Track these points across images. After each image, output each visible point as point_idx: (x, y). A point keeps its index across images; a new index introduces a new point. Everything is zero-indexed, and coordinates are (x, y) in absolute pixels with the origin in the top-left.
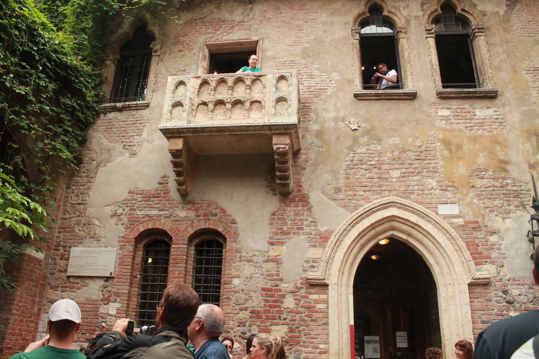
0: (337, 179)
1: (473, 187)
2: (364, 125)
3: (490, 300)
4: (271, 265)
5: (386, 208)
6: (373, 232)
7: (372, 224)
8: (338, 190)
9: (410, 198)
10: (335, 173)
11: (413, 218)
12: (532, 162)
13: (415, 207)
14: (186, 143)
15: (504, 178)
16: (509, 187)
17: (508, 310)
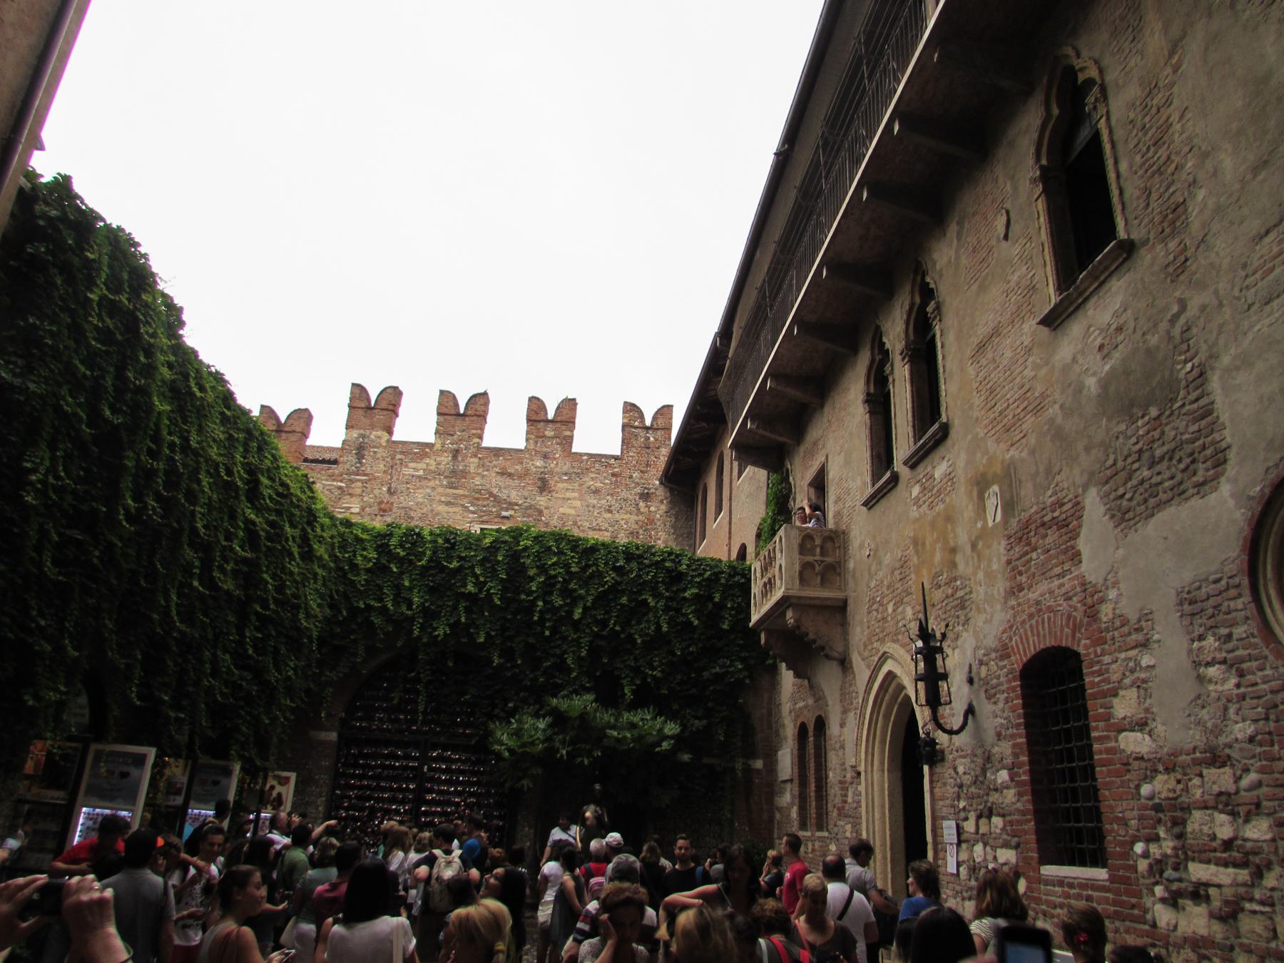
0: (863, 631)
1: (933, 605)
2: (873, 546)
3: (945, 784)
4: (840, 753)
5: (885, 661)
6: (887, 698)
7: (881, 686)
8: (865, 646)
9: (897, 641)
10: (861, 622)
11: (898, 671)
12: (973, 538)
13: (896, 656)
14: (769, 633)
15: (955, 579)
16: (960, 594)
17: (959, 798)
